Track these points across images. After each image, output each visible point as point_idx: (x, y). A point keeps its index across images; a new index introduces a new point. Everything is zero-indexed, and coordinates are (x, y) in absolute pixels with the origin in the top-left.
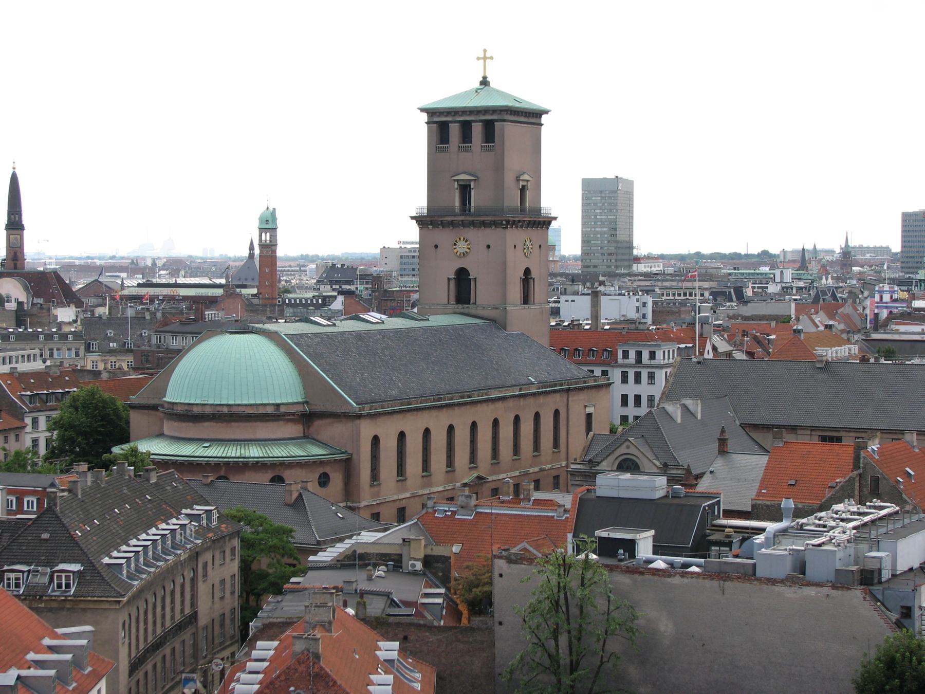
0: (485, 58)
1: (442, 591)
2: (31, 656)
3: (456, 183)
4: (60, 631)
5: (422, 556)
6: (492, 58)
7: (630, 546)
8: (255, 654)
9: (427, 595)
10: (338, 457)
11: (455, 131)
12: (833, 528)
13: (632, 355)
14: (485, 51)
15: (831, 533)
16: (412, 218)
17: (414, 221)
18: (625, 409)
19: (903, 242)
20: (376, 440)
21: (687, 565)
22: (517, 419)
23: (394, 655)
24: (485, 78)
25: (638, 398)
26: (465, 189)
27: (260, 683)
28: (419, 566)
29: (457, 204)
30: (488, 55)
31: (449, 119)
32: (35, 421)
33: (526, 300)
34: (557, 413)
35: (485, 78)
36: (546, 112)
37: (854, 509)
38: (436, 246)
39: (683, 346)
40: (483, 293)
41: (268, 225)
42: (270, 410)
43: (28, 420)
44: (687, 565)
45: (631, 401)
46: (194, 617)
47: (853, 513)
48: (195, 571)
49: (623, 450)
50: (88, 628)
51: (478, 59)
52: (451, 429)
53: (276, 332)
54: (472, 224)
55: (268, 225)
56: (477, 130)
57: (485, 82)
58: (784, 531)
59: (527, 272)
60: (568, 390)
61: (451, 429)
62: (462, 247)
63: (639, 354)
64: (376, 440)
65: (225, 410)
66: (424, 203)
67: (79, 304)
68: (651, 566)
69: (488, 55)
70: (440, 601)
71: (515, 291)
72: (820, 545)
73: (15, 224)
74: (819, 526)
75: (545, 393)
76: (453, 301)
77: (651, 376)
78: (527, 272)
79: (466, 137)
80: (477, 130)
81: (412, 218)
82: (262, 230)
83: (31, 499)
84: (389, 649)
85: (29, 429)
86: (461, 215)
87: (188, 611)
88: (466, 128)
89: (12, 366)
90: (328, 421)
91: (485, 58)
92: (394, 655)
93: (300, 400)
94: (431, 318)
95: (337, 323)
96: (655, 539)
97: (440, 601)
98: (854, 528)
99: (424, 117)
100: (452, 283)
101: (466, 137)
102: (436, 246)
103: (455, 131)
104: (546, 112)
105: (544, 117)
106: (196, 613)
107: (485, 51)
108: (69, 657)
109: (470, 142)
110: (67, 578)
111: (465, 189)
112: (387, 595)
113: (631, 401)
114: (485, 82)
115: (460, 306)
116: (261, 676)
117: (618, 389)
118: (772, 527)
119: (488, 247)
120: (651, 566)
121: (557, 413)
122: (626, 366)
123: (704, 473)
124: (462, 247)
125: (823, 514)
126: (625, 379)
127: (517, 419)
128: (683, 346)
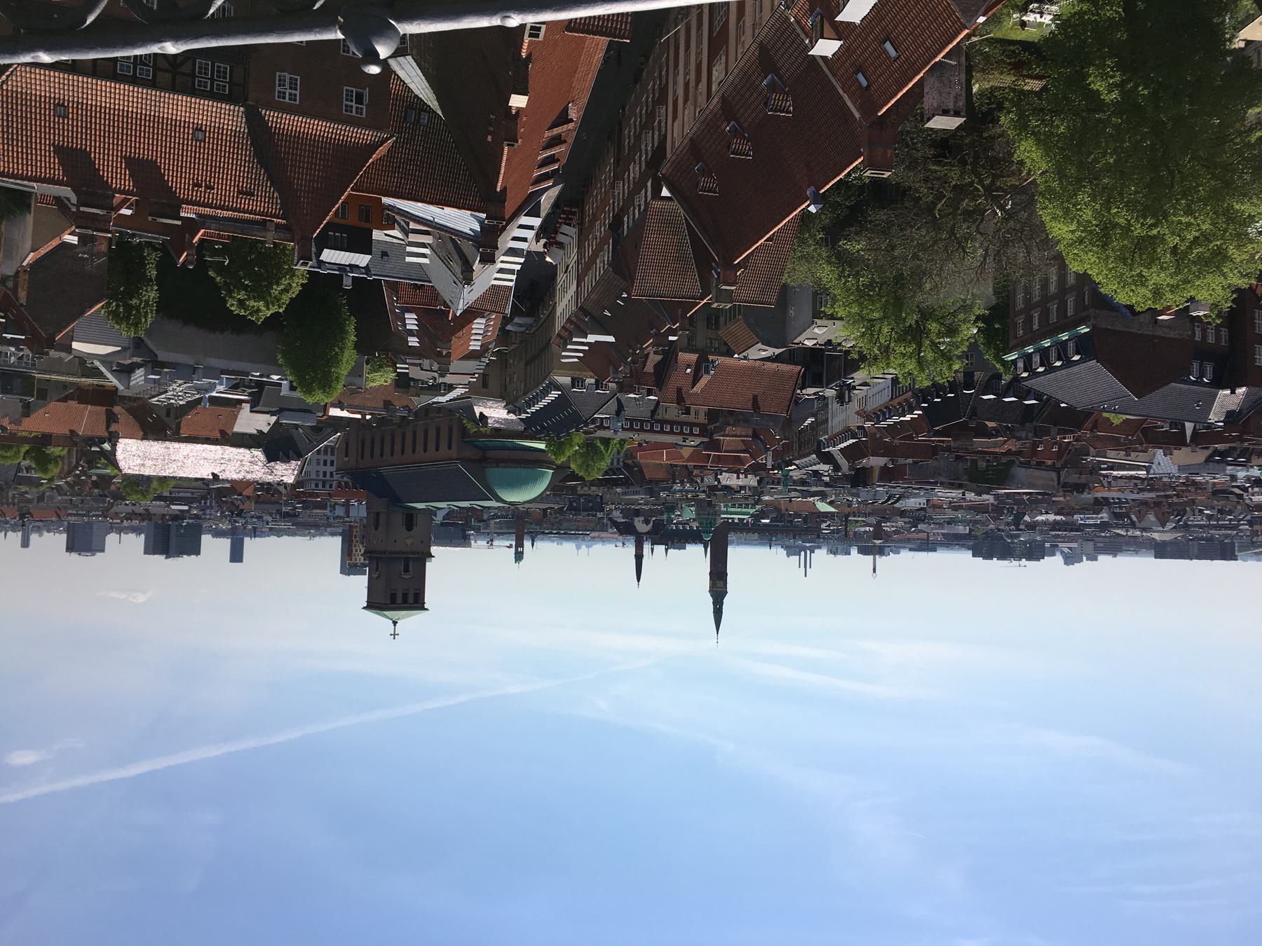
0: (394, 635)
1: (398, 370)
2: (587, 348)
3: (411, 573)
4: (576, 360)
5: (411, 389)
6: (391, 635)
7: (292, 388)
8: (479, 343)
9: (406, 368)
10: (468, 439)
11: (411, 599)
12: (180, 392)
13: (328, 486)
14: (394, 638)
15: (181, 389)
16: (434, 557)
17: (433, 555)
18: (325, 459)
19: (200, 540)
20: (450, 448)
21: (261, 376)
22: (382, 455)
23: (410, 339)
24: (395, 625)
25: (325, 464)
26: (406, 570)
27: (473, 329)
28: (412, 384)
29: (411, 563)
30: (393, 636)
31: (413, 605)
32: (618, 463)
33: (378, 514)
34: (362, 458)
35: (395, 625)
36: (364, 608)
37: (172, 401)
38: (422, 542)
39: (301, 490)
40: (398, 519)
41: (519, 556)
42: (501, 465)
43: (621, 464)
44: (261, 376)
45: (329, 463)
46: (526, 365)
47: (173, 399)
48: (525, 387)
49: (319, 438)
50: (563, 361)
51: (398, 634)
52: (414, 452)
53: (498, 502)
54: (403, 553)
55: (519, 556)
56: (399, 600)
57: (395, 623)
58: (207, 391)
59: (376, 529)
60: (357, 469)
61: (414, 452)
62: (409, 542)
63: (324, 486)
64: (450, 448)
65: (523, 465)
66: (428, 564)
67: (610, 519)
68: (279, 377)
69: (393, 636)
70: (398, 365)
71: (382, 518)
72: (185, 383)
73: (639, 558)
74: (189, 393)
75: (368, 468)
76: (415, 515)
77: (318, 475)
78: (376, 529)
79: (405, 596)
80: (399, 600)
81: (434, 557)
82: (522, 553)
83: (606, 426)
84: (413, 341)
85: (621, 460)
86: (408, 558)
87: (529, 368)
88: (405, 601)
89: (627, 490)
90: (474, 458)
91: (394, 635)
92: (410, 339)
93: (487, 469)
94: (424, 507)
95: (469, 506)
96: (281, 391)
97: (398, 365)
98: (166, 392)
99: (426, 606)
100: (415, 524)
101: (405, 596)
102: (422, 542)
103: (411, 599)
104: (364, 608)
105: (365, 605)
106: (525, 365)
107: (394, 638)
108: (569, 347)
109: (403, 594)
110: (578, 386)
111: (406, 570)
112: (422, 369)
113: (329, 463)
114: (395, 623)
115: (412, 512)
116: (473, 332)
117: (333, 469)
118: (214, 394)
119: (395, 541)
120: (279, 377)
121: (362, 458)
122: (330, 480)
123: (273, 424)
124: (409, 542)
125: (189, 399)
126: (331, 473)
127: (382, 455)
128: (301, 490)
